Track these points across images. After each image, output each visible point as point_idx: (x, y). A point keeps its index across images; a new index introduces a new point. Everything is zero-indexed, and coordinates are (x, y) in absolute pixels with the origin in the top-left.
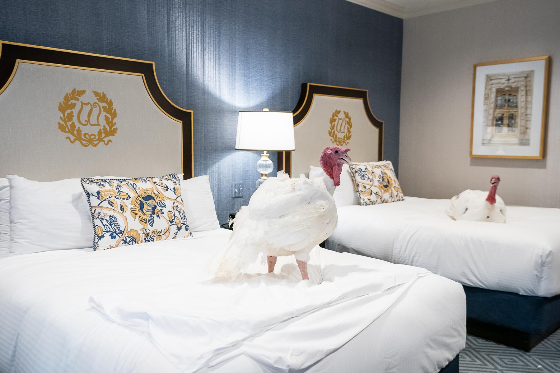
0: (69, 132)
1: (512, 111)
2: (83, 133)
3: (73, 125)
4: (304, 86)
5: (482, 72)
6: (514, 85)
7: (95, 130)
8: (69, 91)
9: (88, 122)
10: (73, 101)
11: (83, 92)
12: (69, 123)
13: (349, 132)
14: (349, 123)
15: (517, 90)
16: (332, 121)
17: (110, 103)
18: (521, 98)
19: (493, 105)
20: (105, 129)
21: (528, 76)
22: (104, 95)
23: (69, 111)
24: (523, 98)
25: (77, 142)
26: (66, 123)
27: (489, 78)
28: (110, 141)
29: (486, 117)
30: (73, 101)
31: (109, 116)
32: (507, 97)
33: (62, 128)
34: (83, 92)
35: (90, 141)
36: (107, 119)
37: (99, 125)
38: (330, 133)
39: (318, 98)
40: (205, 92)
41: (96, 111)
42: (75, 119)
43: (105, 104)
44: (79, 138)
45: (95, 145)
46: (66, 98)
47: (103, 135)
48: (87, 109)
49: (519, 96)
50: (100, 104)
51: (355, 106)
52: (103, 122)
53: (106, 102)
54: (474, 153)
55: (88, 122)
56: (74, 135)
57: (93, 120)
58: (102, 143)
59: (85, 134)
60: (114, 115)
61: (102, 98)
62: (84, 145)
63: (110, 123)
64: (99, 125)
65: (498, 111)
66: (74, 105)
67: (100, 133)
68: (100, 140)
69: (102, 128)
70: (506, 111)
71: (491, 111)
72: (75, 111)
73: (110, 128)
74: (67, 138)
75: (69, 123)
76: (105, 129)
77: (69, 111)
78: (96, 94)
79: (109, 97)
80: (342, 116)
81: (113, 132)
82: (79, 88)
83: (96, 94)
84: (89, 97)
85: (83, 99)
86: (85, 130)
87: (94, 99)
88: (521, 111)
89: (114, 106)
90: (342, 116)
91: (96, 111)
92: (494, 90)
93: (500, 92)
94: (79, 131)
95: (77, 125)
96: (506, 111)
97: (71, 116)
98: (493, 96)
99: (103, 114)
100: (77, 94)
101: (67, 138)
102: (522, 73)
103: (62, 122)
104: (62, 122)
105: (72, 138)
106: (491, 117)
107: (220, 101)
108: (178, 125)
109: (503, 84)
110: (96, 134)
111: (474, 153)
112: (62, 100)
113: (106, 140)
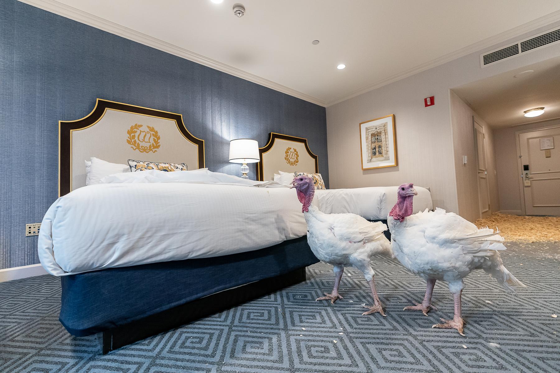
1: (380, 144)
2: (141, 145)
3: (135, 141)
4: (270, 134)
5: (363, 127)
6: (379, 131)
7: (148, 145)
8: (134, 125)
9: (144, 140)
10: (136, 130)
11: (141, 126)
12: (133, 140)
13: (297, 159)
14: (297, 154)
15: (380, 133)
16: (287, 152)
17: (157, 132)
18: (383, 136)
19: (370, 142)
21: (385, 125)
22: (153, 128)
23: (133, 134)
24: (384, 137)
26: (131, 139)
27: (367, 129)
28: (156, 151)
29: (368, 149)
30: (136, 130)
32: (376, 137)
33: (129, 142)
34: (141, 126)
35: (145, 150)
36: (154, 140)
38: (285, 158)
39: (277, 140)
40: (213, 133)
41: (148, 136)
42: (136, 138)
43: (153, 133)
44: (138, 147)
46: (132, 128)
48: (143, 134)
49: (382, 136)
50: (151, 133)
51: (300, 147)
52: (152, 141)
54: (364, 168)
55: (144, 140)
56: (135, 146)
57: (147, 139)
59: (142, 147)
60: (159, 138)
61: (152, 129)
63: (156, 142)
65: (373, 145)
70: (377, 144)
71: (370, 145)
72: (137, 135)
75: (133, 140)
77: (133, 134)
78: (148, 127)
79: (156, 129)
80: (292, 150)
83: (148, 127)
85: (141, 129)
87: (147, 130)
88: (383, 143)
89: (159, 134)
90: (292, 150)
91: (148, 136)
92: (370, 135)
93: (373, 135)
96: (377, 144)
97: (134, 136)
98: (370, 137)
100: (137, 126)
102: (382, 124)
106: (370, 148)
107: (222, 138)
108: (196, 147)
109: (374, 131)
111: (364, 168)
112: (129, 129)
113: (154, 150)
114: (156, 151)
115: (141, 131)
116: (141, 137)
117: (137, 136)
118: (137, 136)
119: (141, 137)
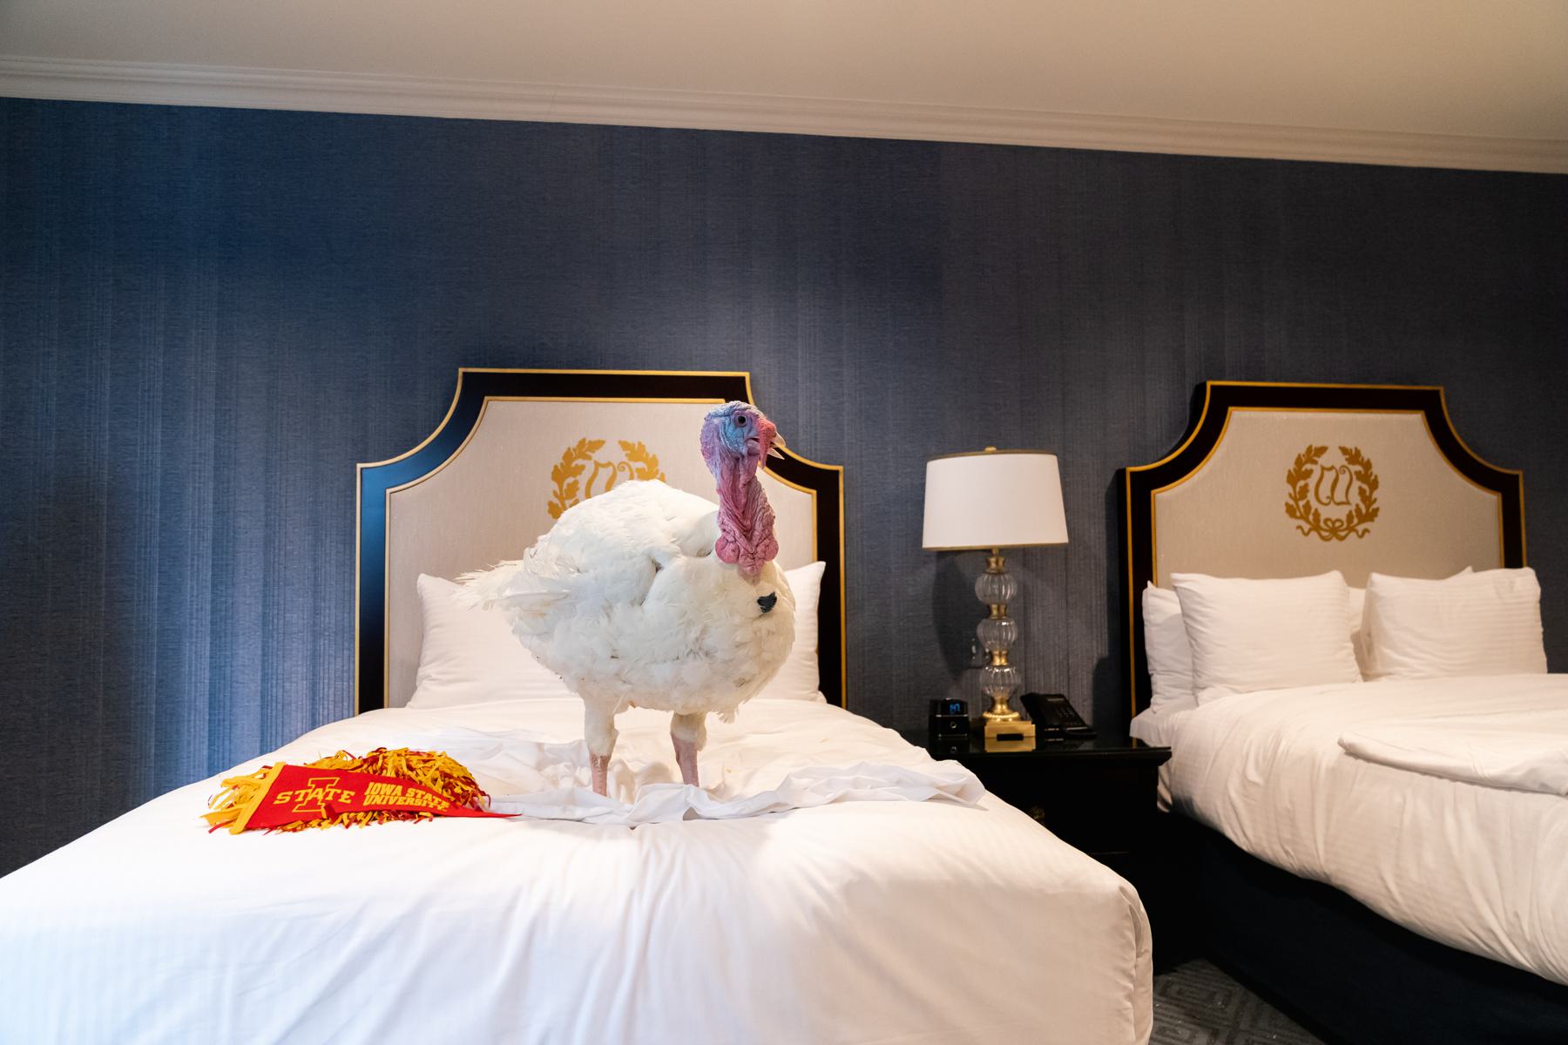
0: (1301, 517)
2: (1322, 518)
3: (1308, 507)
8: (1303, 451)
9: (1331, 498)
11: (1322, 450)
12: (1301, 503)
20: (1358, 509)
22: (1358, 452)
23: (1302, 483)
25: (1314, 534)
26: (1296, 500)
28: (1366, 531)
30: (1308, 466)
31: (1365, 487)
33: (1291, 511)
34: (1322, 450)
35: (1334, 531)
37: (1348, 503)
41: (1344, 480)
42: (1311, 496)
43: (1358, 468)
44: (1316, 527)
45: (1342, 539)
47: (1356, 521)
52: (1355, 498)
53: (1361, 464)
55: (1331, 498)
56: (1308, 521)
57: (1340, 495)
58: (1353, 534)
59: (1326, 520)
60: (1374, 485)
61: (1353, 456)
62: (1323, 538)
63: (1367, 499)
64: (1348, 503)
66: (1309, 473)
67: (1350, 517)
68: (1351, 529)
69: (1353, 508)
72: (1312, 482)
73: (1368, 507)
74: (1299, 527)
75: (1301, 503)
76: (1358, 509)
77: (1302, 483)
78: (1344, 450)
79: (1365, 454)
81: (1371, 515)
82: (1317, 444)
83: (1344, 450)
84: (1334, 458)
85: (1323, 460)
86: (1327, 512)
87: (1340, 460)
89: (1375, 470)
91: (1344, 480)
94: (1317, 514)
95: (1314, 504)
97: (1305, 490)
99: (1356, 484)
100: (1315, 453)
101: (1299, 527)
103: (1291, 502)
104: (1291, 502)
105: (1306, 527)
110: (1344, 518)
112: (1292, 466)
113: (1360, 528)
114: (1366, 531)
115: (1323, 469)
116: (1325, 490)
117: (1312, 487)
118: (1312, 487)
119: (1325, 490)
